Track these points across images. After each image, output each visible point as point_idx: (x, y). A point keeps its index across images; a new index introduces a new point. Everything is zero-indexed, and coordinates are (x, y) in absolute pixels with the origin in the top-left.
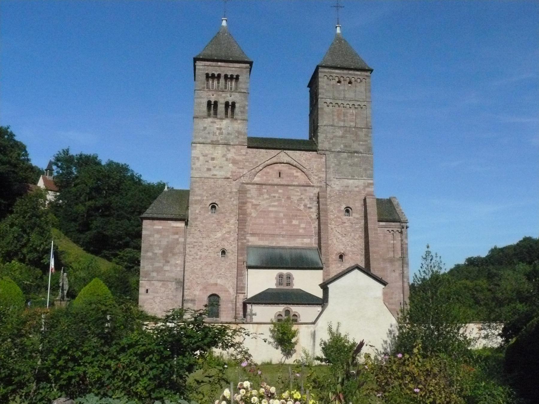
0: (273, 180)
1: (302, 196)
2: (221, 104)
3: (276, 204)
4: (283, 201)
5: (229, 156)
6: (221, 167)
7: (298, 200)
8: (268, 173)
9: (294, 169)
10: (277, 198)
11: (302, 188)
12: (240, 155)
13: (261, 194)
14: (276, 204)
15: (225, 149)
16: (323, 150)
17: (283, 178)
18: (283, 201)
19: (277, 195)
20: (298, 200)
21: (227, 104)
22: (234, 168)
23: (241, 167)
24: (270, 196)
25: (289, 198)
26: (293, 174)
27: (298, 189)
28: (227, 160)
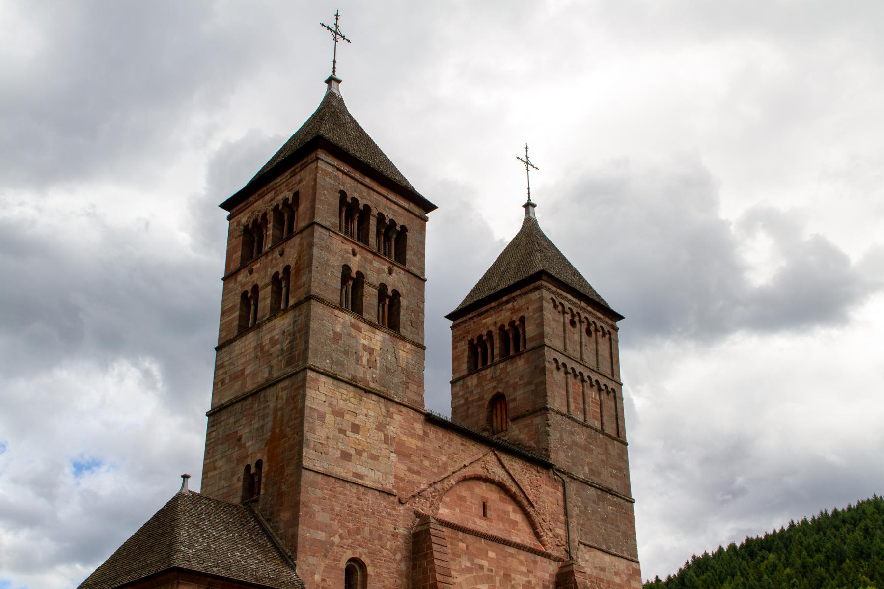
0: (475, 523)
1: (531, 578)
2: (371, 285)
5: (391, 430)
8: (462, 499)
12: (413, 435)
15: (383, 410)
17: (491, 520)
21: (382, 289)
22: (402, 469)
23: (416, 468)
27: (523, 556)
28: (387, 440)
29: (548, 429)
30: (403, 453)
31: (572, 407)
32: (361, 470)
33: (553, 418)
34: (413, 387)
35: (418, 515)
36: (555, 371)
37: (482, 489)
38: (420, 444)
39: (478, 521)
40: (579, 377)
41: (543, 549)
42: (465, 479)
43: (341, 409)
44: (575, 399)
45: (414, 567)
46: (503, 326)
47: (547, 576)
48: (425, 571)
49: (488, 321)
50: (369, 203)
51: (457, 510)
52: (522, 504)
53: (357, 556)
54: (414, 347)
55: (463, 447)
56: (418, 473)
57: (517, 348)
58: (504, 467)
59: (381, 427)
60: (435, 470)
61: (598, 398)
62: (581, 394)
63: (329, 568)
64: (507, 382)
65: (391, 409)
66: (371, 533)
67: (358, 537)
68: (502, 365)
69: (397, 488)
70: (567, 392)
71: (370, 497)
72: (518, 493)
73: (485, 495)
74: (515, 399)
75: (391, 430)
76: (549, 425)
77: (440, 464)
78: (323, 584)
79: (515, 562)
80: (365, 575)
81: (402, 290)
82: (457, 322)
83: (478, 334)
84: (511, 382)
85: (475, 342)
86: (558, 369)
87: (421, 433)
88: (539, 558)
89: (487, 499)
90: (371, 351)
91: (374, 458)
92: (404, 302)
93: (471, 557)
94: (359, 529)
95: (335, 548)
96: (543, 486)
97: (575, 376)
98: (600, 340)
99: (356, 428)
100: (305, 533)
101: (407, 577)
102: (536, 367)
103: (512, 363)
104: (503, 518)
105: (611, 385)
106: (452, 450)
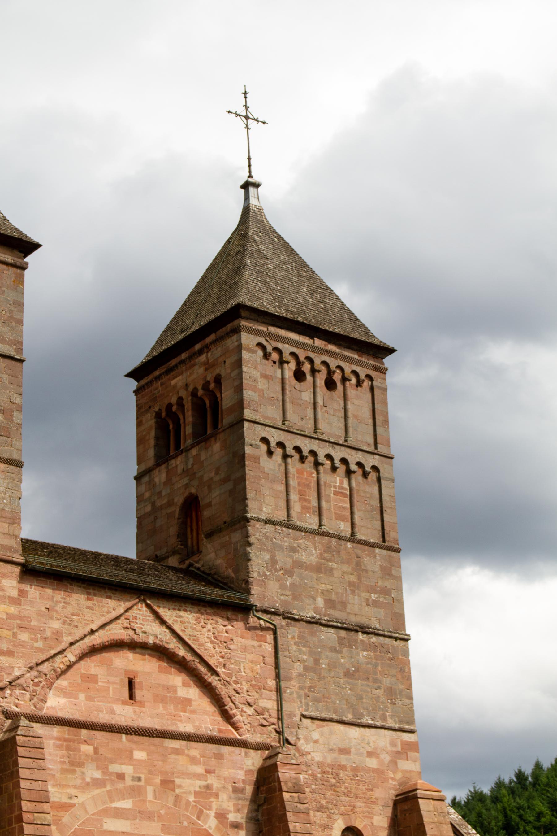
0: (112, 712)
1: (212, 780)
3: (126, 804)
4: (150, 796)
7: (196, 794)
8: (90, 679)
10: (129, 782)
13: (74, 764)
14: (126, 804)
16: (265, 611)
17: (142, 704)
18: (150, 796)
19: (128, 770)
20: (196, 794)
24: (105, 771)
25: (167, 784)
26: (173, 689)
29: (249, 549)
31: (296, 508)
33: (256, 532)
36: (264, 458)
37: (126, 660)
40: (311, 459)
41: (235, 735)
42: (94, 651)
44: (301, 494)
46: (195, 390)
47: (240, 775)
49: (178, 381)
51: (82, 696)
55: (89, 603)
56: (10, 653)
57: (215, 425)
58: (163, 622)
60: (40, 644)
61: (346, 485)
62: (314, 484)
64: (201, 478)
68: (194, 451)
70: (287, 485)
72: (189, 657)
73: (131, 667)
74: (209, 505)
76: (250, 544)
77: (48, 634)
79: (182, 761)
82: (143, 382)
84: (206, 478)
85: (164, 415)
86: (270, 453)
88: (226, 750)
89: (136, 673)
96: (237, 640)
97: (302, 459)
103: (206, 448)
104: (165, 696)
105: (369, 461)
106: (70, 609)
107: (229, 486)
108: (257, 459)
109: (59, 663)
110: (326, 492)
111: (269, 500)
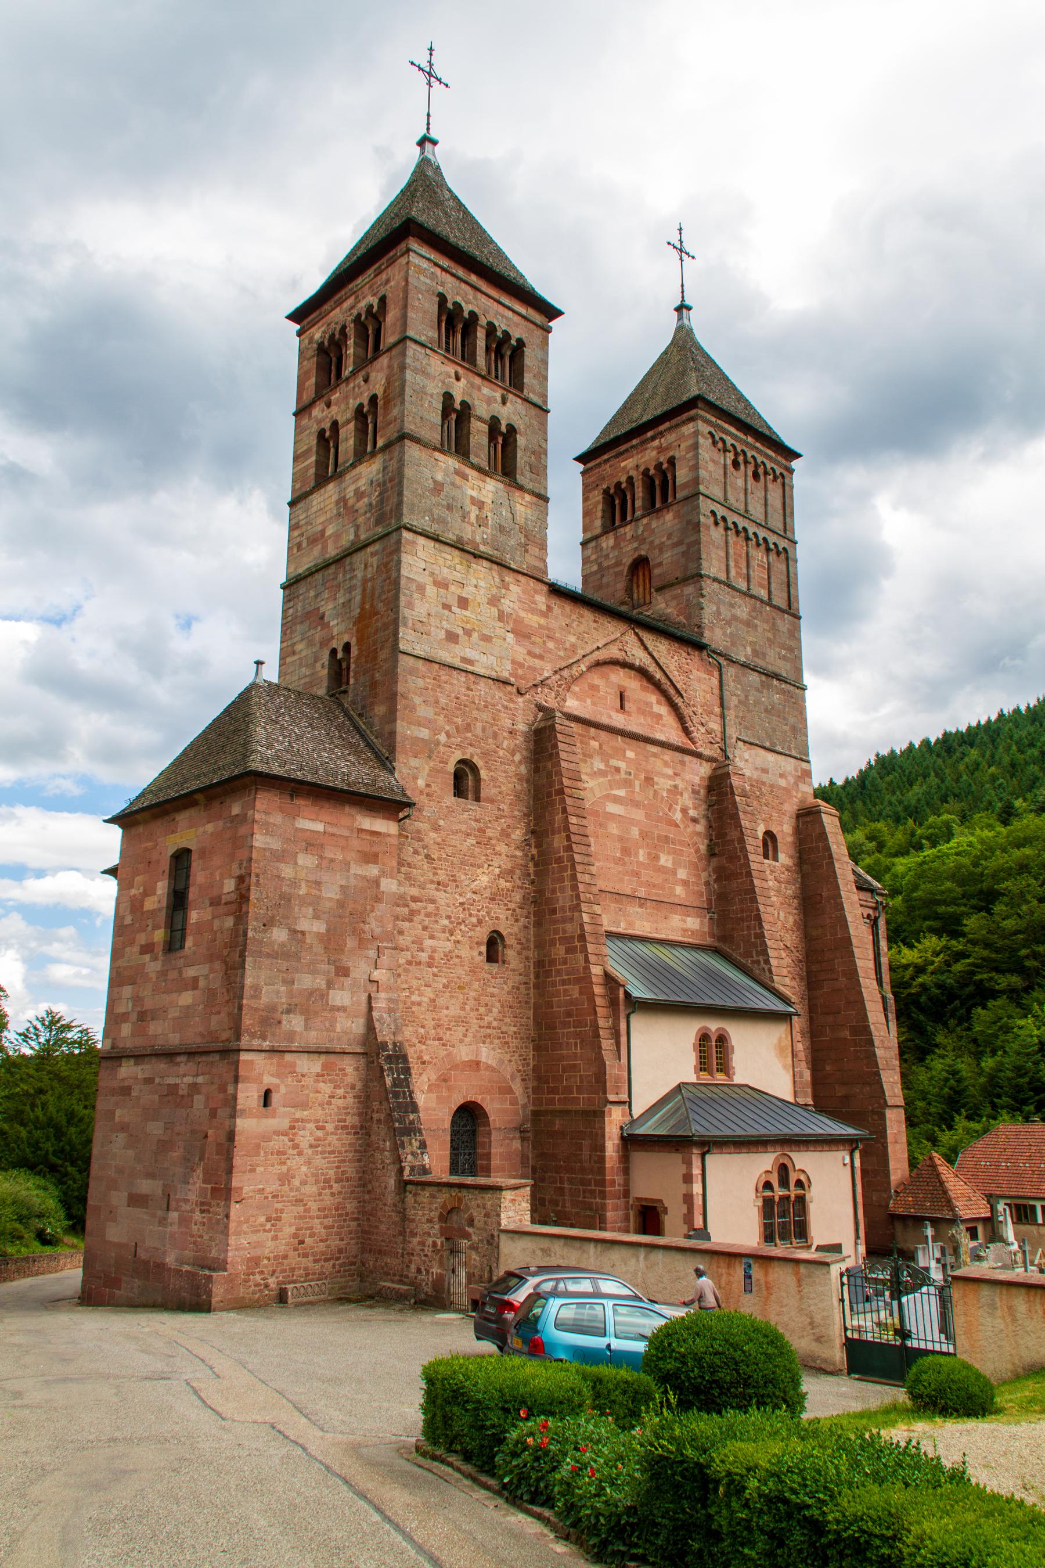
0: (610, 717)
2: (480, 419)
5: (507, 605)
6: (486, 639)
8: (594, 688)
9: (653, 693)
11: (678, 756)
15: (497, 580)
17: (629, 714)
21: (494, 424)
22: (520, 652)
23: (537, 651)
25: (649, 780)
27: (668, 755)
28: (501, 617)
30: (521, 633)
31: (733, 573)
32: (470, 654)
33: (709, 587)
34: (534, 550)
35: (540, 708)
36: (713, 527)
37: (619, 677)
38: (543, 621)
39: (614, 715)
40: (743, 534)
42: (598, 664)
43: (444, 579)
45: (537, 770)
48: (549, 775)
50: (476, 310)
51: (589, 701)
52: (668, 693)
53: (467, 757)
54: (535, 499)
56: (541, 657)
57: (665, 499)
58: (646, 648)
59: (494, 601)
60: (562, 653)
63: (434, 772)
64: (652, 542)
65: (507, 579)
66: (484, 729)
67: (469, 735)
68: (645, 521)
69: (516, 676)
70: (727, 553)
71: (482, 686)
72: (664, 680)
73: (622, 683)
75: (507, 605)
76: (703, 596)
77: (567, 646)
78: (427, 790)
79: (659, 763)
80: (478, 780)
81: (519, 424)
83: (615, 481)
84: (657, 542)
85: (612, 491)
86: (716, 524)
87: (544, 608)
89: (625, 688)
90: (481, 505)
91: (486, 639)
92: (521, 441)
93: (605, 758)
94: (469, 725)
95: (442, 748)
97: (738, 533)
98: (770, 486)
99: (463, 603)
100: (404, 729)
101: (528, 781)
102: (688, 522)
104: (644, 710)
106: (582, 628)
107: (683, 548)
108: (708, 528)
109: (575, 671)
110: (754, 563)
111: (715, 562)
